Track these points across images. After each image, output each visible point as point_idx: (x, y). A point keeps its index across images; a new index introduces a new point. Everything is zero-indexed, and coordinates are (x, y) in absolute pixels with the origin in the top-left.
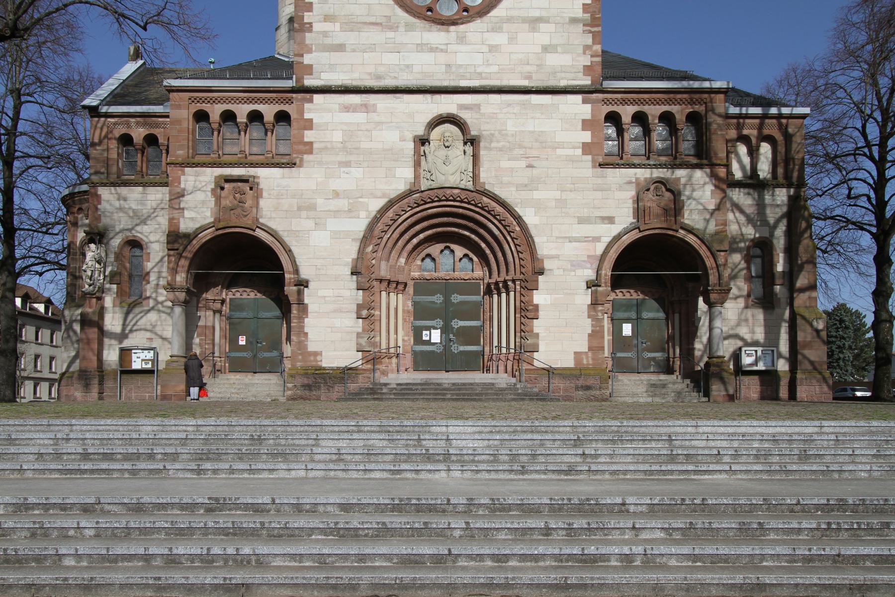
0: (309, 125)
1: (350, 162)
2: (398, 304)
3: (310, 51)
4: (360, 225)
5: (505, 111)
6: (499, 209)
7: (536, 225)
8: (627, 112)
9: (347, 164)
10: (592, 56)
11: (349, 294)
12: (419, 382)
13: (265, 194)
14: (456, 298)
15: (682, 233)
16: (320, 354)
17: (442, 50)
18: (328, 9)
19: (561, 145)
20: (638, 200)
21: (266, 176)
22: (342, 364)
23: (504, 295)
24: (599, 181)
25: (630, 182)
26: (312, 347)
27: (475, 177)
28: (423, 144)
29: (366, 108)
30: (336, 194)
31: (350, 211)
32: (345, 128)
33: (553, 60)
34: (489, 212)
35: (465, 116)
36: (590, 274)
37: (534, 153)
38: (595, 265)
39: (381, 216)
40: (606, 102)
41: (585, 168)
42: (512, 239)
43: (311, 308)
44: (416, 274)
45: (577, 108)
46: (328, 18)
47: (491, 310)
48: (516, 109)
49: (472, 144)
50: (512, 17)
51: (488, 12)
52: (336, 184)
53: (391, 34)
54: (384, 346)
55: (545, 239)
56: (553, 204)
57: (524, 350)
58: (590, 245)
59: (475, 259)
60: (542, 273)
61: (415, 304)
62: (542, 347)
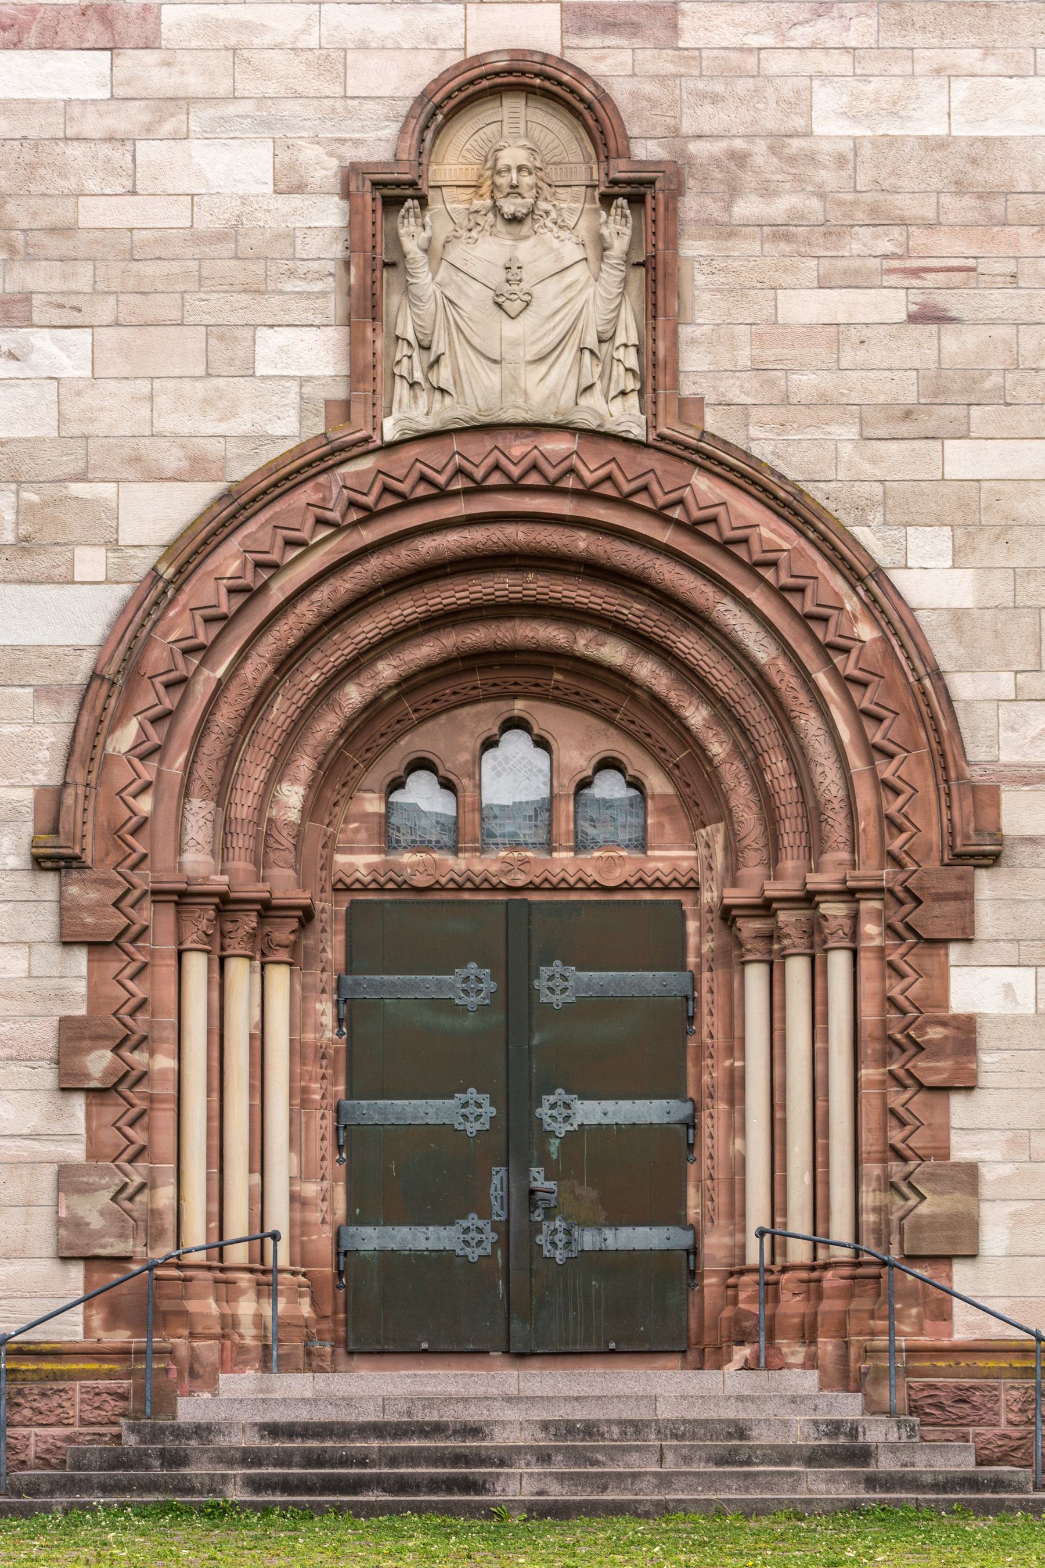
1: (26, 298)
4: (75, 617)
5: (802, 35)
6: (772, 532)
7: (958, 616)
12: (371, 1415)
14: (561, 983)
23: (797, 970)
27: (656, 373)
28: (392, 204)
31: (25, 545)
34: (724, 547)
35: (609, 64)
37: (950, 248)
39: (184, 573)
42: (845, 682)
44: (359, 862)
47: (736, 1044)
49: (636, 201)
54: (196, 1232)
55: (1005, 683)
57: (904, 1260)
59: (657, 783)
60: (992, 859)
62: (994, 1238)
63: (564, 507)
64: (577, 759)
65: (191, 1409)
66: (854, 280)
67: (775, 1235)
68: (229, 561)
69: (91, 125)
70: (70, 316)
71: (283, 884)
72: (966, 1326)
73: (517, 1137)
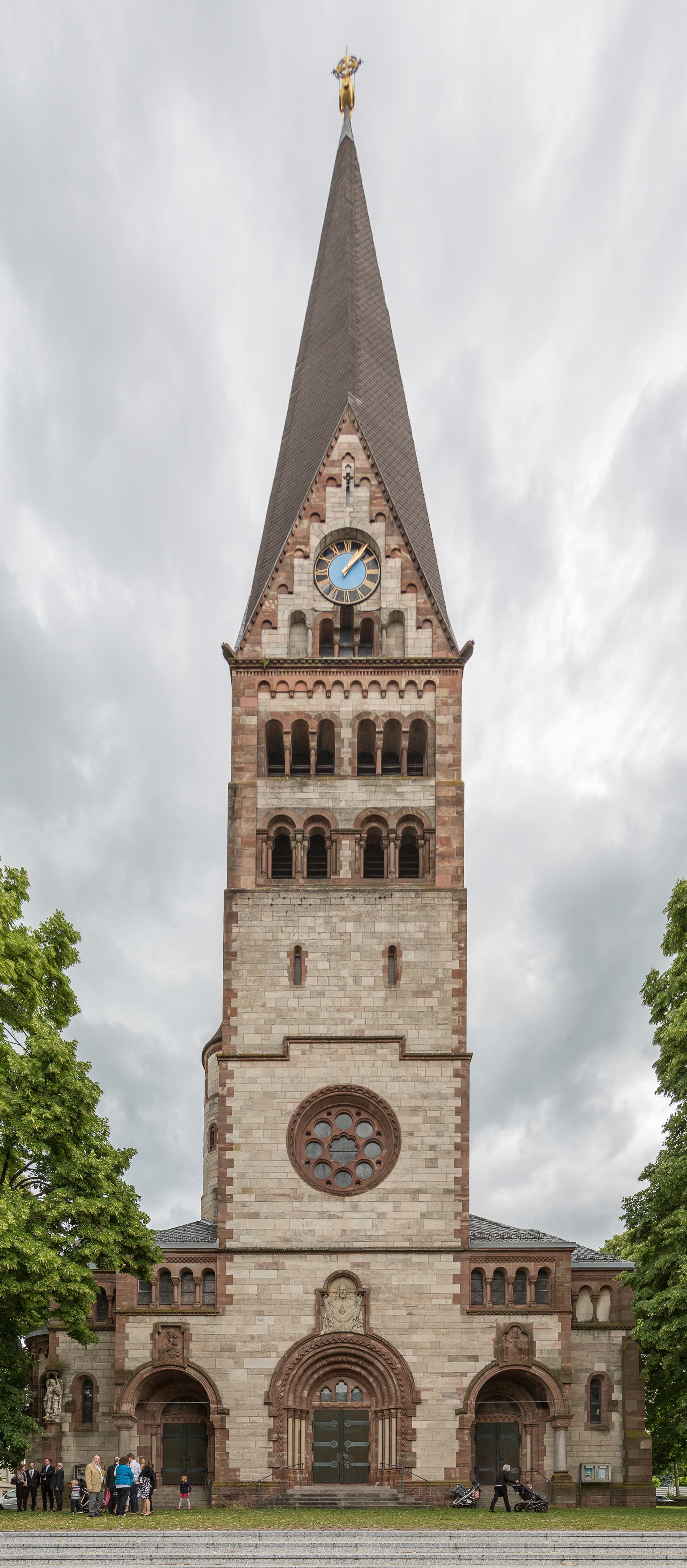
0: (230, 1280)
2: (302, 1427)
3: (231, 1219)
4: (271, 1363)
5: (390, 1267)
6: (384, 1350)
7: (414, 1363)
8: (489, 1269)
9: (261, 1313)
10: (462, 1221)
11: (262, 1420)
13: (194, 1338)
14: (348, 1423)
15: (534, 1370)
16: (239, 1470)
17: (339, 1217)
18: (246, 1183)
19: (436, 1296)
20: (498, 1341)
21: (196, 1324)
22: (257, 1479)
23: (387, 1421)
24: (466, 1326)
25: (491, 1327)
26: (232, 1465)
27: (366, 1323)
28: (323, 1295)
29: (276, 1266)
30: (252, 1338)
31: (263, 1352)
32: (259, 1282)
33: (430, 1225)
34: (376, 1352)
35: (358, 1272)
36: (458, 1403)
37: (414, 1303)
38: (462, 1397)
40: (472, 1260)
41: (455, 1315)
42: (395, 1374)
43: (231, 1432)
45: (451, 1265)
46: (246, 1191)
47: (377, 1433)
48: (399, 1267)
49: (363, 1295)
50: (397, 1189)
51: (377, 1185)
52: (251, 1330)
53: (297, 1204)
54: (290, 1463)
55: (421, 1375)
56: (429, 1345)
58: (457, 1380)
59: (364, 1390)
60: (419, 1403)
61: (314, 1428)
62: (419, 1464)
63: (351, 1346)
64: (351, 1387)
65: (289, 1492)
66: (398, 1308)
67: (383, 1464)
68: (296, 1354)
69: (274, 1282)
70: (270, 1314)
71: (304, 1407)
72: (414, 1478)
73: (341, 1448)
